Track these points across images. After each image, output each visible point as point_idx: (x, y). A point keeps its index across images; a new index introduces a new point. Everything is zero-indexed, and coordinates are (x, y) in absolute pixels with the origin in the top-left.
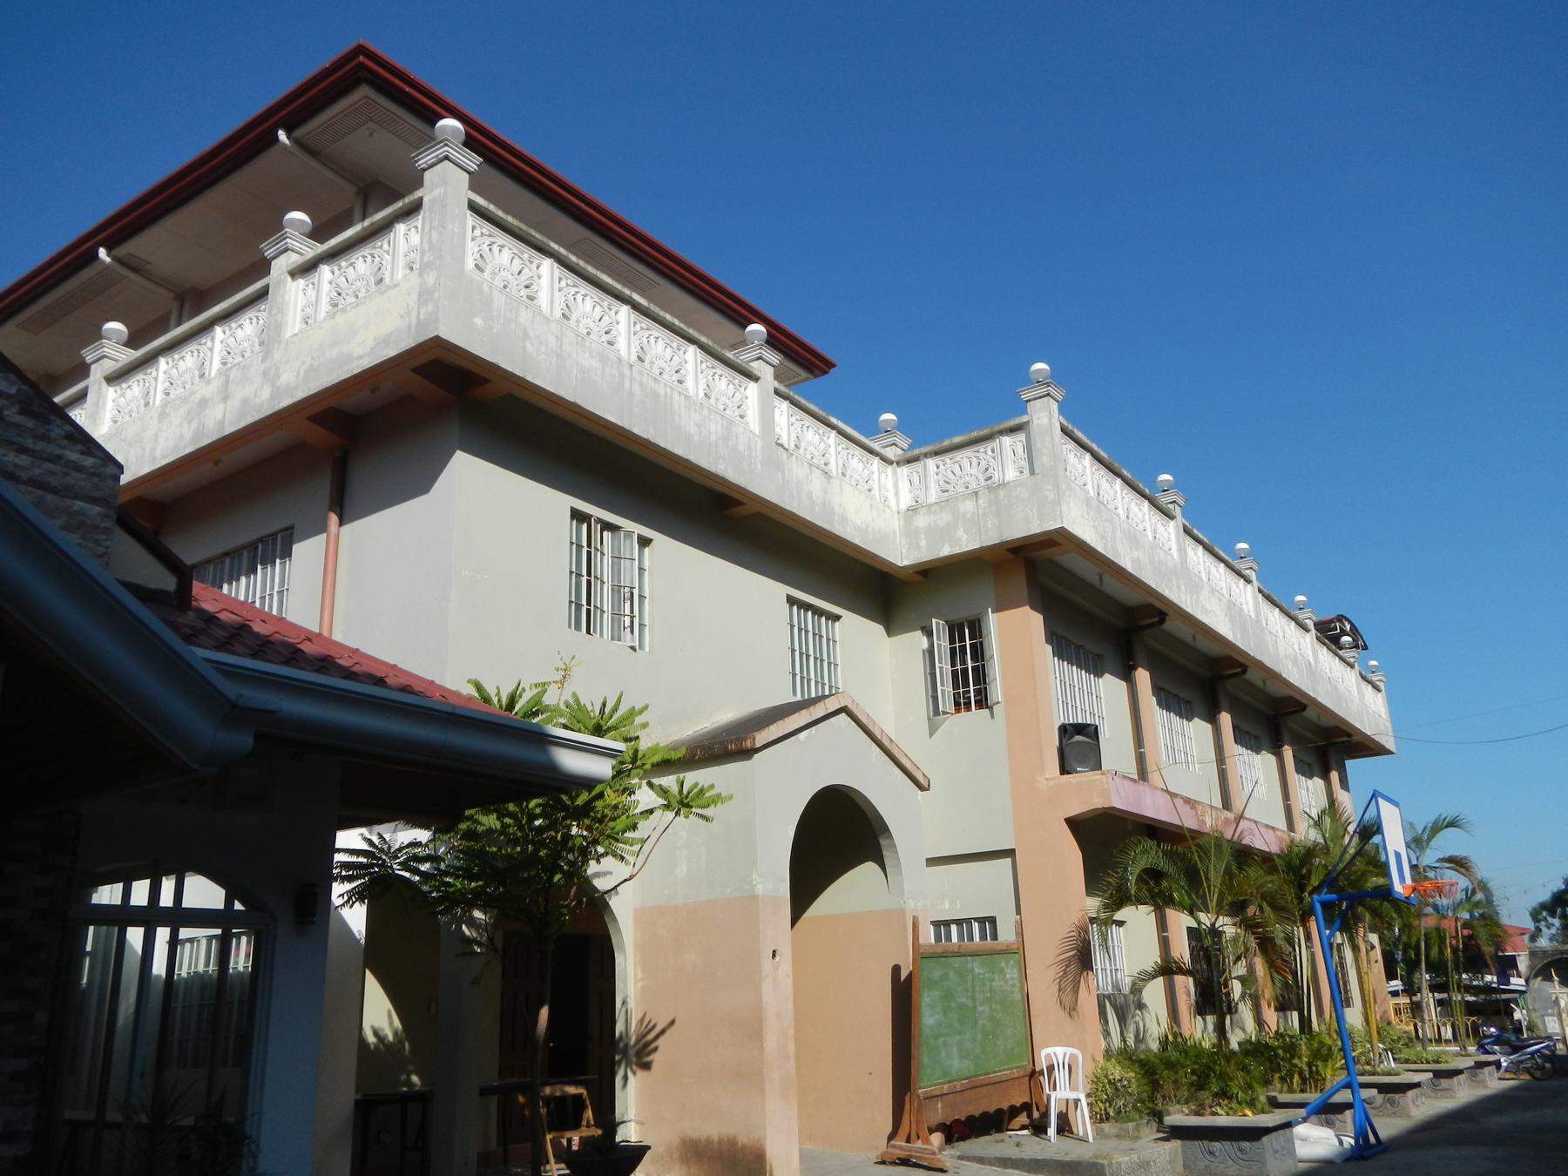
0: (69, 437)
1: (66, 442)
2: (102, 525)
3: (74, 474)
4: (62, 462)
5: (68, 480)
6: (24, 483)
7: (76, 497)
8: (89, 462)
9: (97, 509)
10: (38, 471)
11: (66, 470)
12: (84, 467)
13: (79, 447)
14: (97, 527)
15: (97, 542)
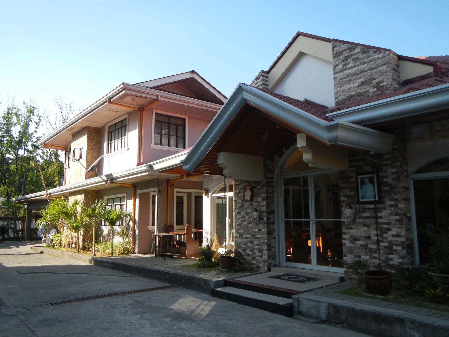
0: (375, 52)
1: (374, 54)
2: (388, 70)
3: (378, 61)
5: (377, 63)
6: (367, 71)
7: (380, 66)
8: (381, 55)
9: (385, 66)
10: (369, 66)
11: (376, 61)
12: (380, 57)
13: (378, 53)
14: (386, 71)
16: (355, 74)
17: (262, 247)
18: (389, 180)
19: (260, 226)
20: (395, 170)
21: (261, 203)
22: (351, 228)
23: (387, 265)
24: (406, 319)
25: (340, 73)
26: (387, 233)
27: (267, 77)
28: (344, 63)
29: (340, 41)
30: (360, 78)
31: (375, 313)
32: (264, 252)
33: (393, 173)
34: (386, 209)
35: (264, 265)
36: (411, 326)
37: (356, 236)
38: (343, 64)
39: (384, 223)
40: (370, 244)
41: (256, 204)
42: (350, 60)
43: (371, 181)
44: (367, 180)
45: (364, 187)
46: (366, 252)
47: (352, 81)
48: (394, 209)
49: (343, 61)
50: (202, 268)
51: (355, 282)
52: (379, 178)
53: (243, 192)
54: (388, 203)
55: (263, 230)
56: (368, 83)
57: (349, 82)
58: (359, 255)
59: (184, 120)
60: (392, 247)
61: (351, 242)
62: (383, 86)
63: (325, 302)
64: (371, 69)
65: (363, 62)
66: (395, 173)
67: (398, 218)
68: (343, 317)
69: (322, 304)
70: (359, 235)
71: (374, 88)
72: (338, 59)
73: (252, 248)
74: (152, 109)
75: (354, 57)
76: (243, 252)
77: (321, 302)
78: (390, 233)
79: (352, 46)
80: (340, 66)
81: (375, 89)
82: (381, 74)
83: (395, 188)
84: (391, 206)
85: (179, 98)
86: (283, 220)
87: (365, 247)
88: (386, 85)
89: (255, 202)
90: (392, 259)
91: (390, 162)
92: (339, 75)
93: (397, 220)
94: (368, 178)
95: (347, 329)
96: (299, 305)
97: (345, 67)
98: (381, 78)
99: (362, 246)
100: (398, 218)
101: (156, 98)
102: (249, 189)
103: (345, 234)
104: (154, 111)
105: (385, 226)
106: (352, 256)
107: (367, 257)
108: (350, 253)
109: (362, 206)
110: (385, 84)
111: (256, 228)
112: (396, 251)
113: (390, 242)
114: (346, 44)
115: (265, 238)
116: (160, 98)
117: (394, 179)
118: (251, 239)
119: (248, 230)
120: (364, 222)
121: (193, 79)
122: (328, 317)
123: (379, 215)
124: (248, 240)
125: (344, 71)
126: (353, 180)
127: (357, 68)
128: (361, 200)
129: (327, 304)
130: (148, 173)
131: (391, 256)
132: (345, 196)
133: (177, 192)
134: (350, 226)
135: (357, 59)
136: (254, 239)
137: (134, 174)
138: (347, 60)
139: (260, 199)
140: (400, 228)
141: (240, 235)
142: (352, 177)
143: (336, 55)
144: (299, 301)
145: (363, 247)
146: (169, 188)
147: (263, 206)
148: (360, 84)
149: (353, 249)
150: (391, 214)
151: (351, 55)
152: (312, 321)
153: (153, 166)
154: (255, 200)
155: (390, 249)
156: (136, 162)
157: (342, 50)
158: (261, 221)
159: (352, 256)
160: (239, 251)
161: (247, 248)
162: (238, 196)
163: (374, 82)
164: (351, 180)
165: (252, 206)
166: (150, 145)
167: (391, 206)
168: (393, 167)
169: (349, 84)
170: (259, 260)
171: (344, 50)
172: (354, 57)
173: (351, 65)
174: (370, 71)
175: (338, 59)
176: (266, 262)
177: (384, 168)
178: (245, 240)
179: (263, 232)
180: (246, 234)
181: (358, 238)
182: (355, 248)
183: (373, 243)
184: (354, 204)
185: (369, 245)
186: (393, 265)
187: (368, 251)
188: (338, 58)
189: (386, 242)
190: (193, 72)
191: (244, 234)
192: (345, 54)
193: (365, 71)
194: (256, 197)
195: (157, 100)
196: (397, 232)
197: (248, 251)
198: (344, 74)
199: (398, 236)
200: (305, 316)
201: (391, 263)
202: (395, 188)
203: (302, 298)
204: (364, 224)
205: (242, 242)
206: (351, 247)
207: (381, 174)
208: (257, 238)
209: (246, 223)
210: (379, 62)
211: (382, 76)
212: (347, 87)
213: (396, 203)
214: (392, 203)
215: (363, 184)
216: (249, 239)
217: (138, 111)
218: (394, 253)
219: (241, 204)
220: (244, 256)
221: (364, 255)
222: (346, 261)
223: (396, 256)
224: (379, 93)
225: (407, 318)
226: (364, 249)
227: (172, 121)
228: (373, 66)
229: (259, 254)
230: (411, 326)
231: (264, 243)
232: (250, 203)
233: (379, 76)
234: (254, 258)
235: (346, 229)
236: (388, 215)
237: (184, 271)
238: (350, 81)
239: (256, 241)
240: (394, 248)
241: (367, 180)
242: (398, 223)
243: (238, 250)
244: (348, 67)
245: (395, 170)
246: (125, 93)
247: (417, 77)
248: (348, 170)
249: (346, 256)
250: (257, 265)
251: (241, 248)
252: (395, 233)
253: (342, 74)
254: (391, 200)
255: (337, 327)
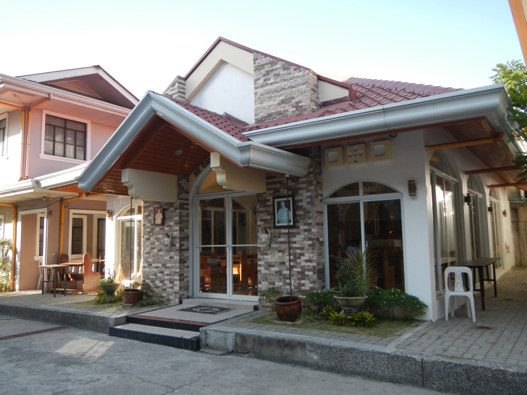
0: (295, 70)
3: (298, 79)
4: (294, 78)
5: (297, 82)
9: (305, 86)
10: (289, 84)
11: (296, 80)
12: (300, 76)
13: (298, 71)
14: (305, 91)
15: (306, 96)
16: (276, 91)
17: (173, 278)
18: (304, 204)
19: (172, 254)
20: (309, 194)
21: (173, 228)
22: (267, 254)
23: (299, 291)
24: (307, 342)
25: (260, 88)
26: (300, 258)
27: (185, 85)
28: (266, 77)
29: (263, 54)
30: (280, 96)
31: (279, 339)
32: (175, 283)
33: (307, 197)
34: (300, 233)
35: (175, 297)
36: (311, 349)
37: (271, 262)
38: (264, 78)
39: (298, 248)
40: (284, 270)
41: (167, 229)
42: (271, 75)
43: (288, 206)
44: (283, 204)
45: (280, 210)
46: (280, 278)
47: (272, 98)
48: (307, 234)
49: (264, 75)
50: (102, 304)
51: (268, 309)
52: (294, 202)
53: (153, 215)
54: (302, 227)
55: (175, 257)
56: (288, 102)
57: (269, 99)
58: (273, 281)
59: (85, 125)
60: (304, 273)
61: (266, 269)
62: (302, 106)
63: (233, 332)
64: (291, 87)
65: (283, 79)
66: (310, 197)
67: (310, 242)
68: (249, 346)
69: (229, 335)
70: (274, 261)
71: (293, 107)
72: (259, 73)
73: (162, 279)
74: (42, 110)
75: (275, 72)
76: (151, 284)
77: (229, 333)
78: (303, 258)
79: (274, 60)
80: (261, 81)
81: (294, 109)
82: (300, 93)
83: (309, 212)
84: (305, 230)
85: (79, 98)
86: (198, 246)
87: (279, 273)
88: (304, 106)
89: (167, 226)
90: (303, 285)
91: (305, 185)
92: (260, 91)
93: (309, 245)
94: (284, 201)
95: (253, 358)
96: (206, 338)
97: (266, 82)
98: (300, 98)
99: (276, 272)
100: (310, 242)
101: (47, 96)
102: (161, 212)
103: (260, 260)
104: (45, 112)
105: (298, 251)
106: (267, 283)
107: (281, 284)
108: (265, 279)
109: (277, 231)
110: (303, 104)
111: (167, 256)
112: (308, 276)
113: (303, 267)
114: (268, 58)
115: (177, 267)
116: (52, 97)
117: (308, 203)
118: (161, 268)
119: (158, 258)
120: (278, 248)
121: (97, 76)
122: (235, 348)
123: (294, 239)
124: (157, 269)
125: (265, 86)
126: (270, 203)
127: (277, 84)
128: (277, 225)
129: (234, 335)
130: (34, 191)
131: (303, 282)
132: (262, 220)
133: (74, 214)
134: (266, 252)
135: (278, 75)
136: (164, 268)
137: (15, 191)
138: (268, 74)
139: (172, 223)
140: (312, 253)
141: (148, 265)
142: (269, 200)
143: (257, 68)
144: (207, 333)
145: (277, 274)
146: (63, 208)
147: (176, 231)
148: (280, 102)
149: (267, 275)
150: (304, 239)
151: (272, 70)
152: (219, 353)
153: (40, 182)
154: (166, 224)
155: (302, 275)
156: (19, 176)
157: (263, 63)
158: (173, 248)
159: (267, 283)
160: (147, 283)
161: (156, 279)
162: (148, 220)
163: (294, 101)
164: (268, 203)
165: (163, 231)
166: (38, 155)
167: (305, 230)
168: (308, 191)
169: (269, 101)
170: (170, 292)
171: (266, 64)
172: (275, 72)
173: (272, 81)
174: (290, 89)
175: (259, 73)
176: (178, 293)
177: (300, 192)
178: (154, 270)
179: (175, 261)
180: (155, 263)
181: (273, 264)
182: (270, 275)
183: (287, 269)
184: (270, 228)
185: (283, 271)
186: (305, 290)
187: (282, 278)
188: (259, 71)
189: (299, 268)
190: (98, 67)
191: (154, 263)
192: (267, 68)
193: (285, 89)
194: (168, 221)
195: (48, 99)
196: (309, 257)
197: (157, 282)
198: (265, 90)
199: (310, 261)
200: (213, 349)
201: (303, 288)
202: (309, 212)
203: (210, 330)
204: (279, 249)
205: (150, 273)
206: (266, 274)
207: (297, 198)
208: (168, 267)
209: (156, 251)
210: (299, 80)
211: (301, 96)
212: (267, 104)
213: (310, 227)
214: (306, 227)
215: (279, 207)
216: (159, 269)
217: (22, 111)
218: (306, 278)
219: (151, 229)
220: (152, 288)
221: (278, 282)
222: (261, 288)
223: (308, 281)
224: (297, 113)
225: (308, 341)
226: (278, 275)
227: (69, 126)
228: (293, 84)
229: (170, 285)
230: (311, 349)
231: (175, 273)
232: (161, 227)
233: (298, 96)
234: (165, 290)
235: (262, 255)
236: (301, 240)
237: (78, 309)
238: (270, 97)
239: (166, 271)
240: (306, 273)
241: (283, 204)
242: (311, 248)
243: (146, 282)
244: (269, 82)
245: (309, 194)
246: (4, 87)
247: (334, 100)
248: (265, 193)
249: (261, 284)
250: (167, 298)
251: (149, 279)
252: (307, 258)
253: (262, 90)
254: (305, 224)
255: (244, 357)
